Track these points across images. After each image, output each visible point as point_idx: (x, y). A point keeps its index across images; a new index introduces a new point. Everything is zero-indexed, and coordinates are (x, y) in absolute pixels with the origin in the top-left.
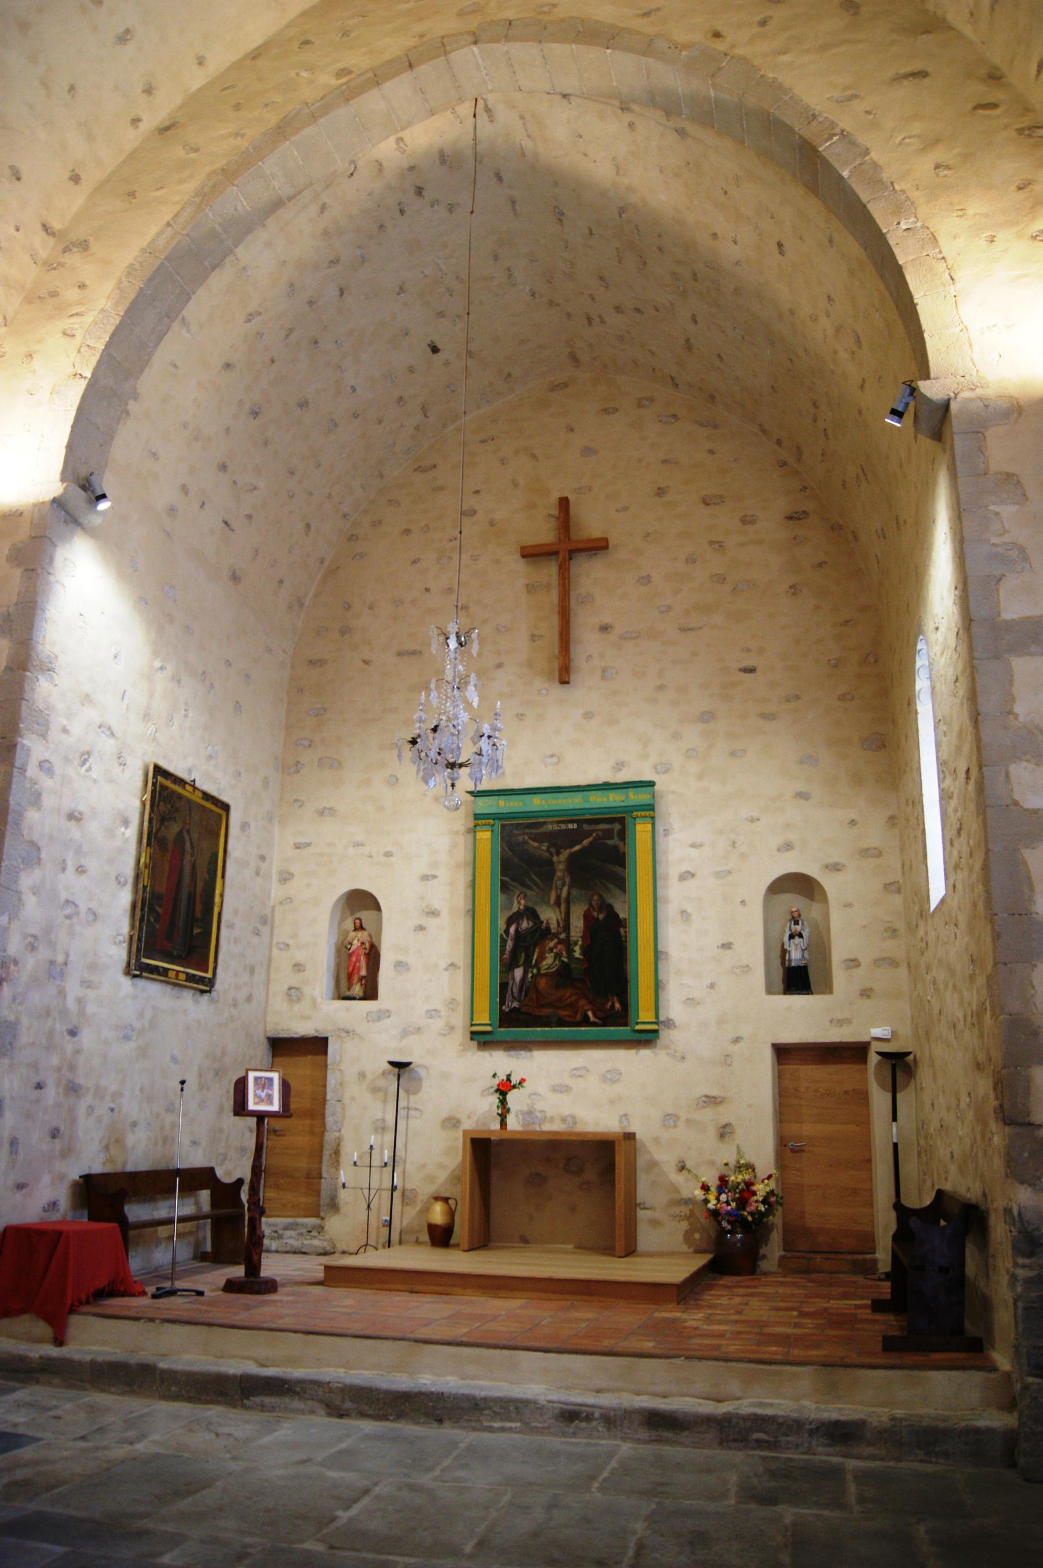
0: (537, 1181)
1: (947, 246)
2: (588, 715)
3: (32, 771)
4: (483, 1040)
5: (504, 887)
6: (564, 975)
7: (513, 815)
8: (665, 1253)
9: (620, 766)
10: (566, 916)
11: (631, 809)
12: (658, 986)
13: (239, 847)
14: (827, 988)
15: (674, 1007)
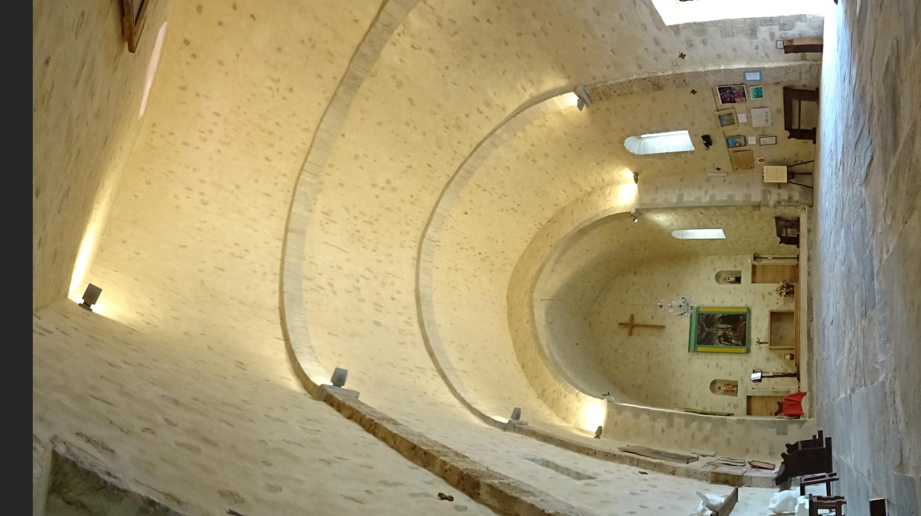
0: (781, 337)
1: (607, 207)
4: (748, 351)
6: (734, 330)
10: (721, 329)
14: (740, 272)
15: (743, 304)
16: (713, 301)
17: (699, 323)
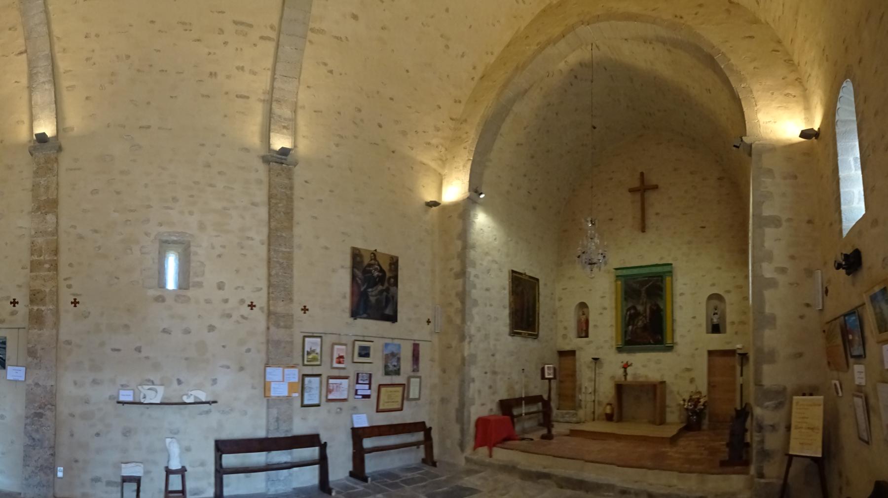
2: (652, 242)
3: (472, 278)
4: (620, 350)
5: (626, 299)
6: (645, 328)
7: (627, 276)
8: (674, 417)
9: (662, 258)
11: (664, 273)
12: (673, 331)
13: (544, 291)
15: (678, 339)
16: (682, 294)
17: (651, 276)
